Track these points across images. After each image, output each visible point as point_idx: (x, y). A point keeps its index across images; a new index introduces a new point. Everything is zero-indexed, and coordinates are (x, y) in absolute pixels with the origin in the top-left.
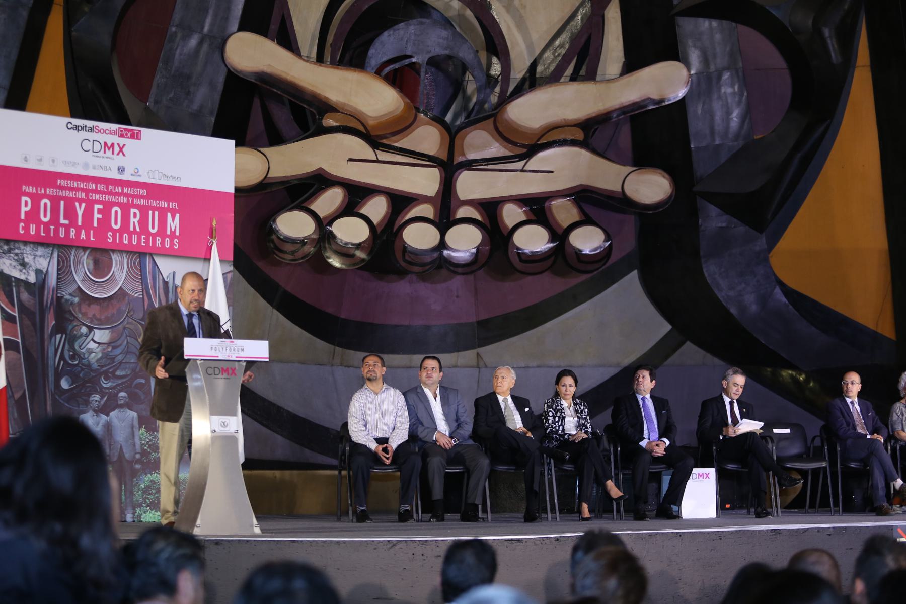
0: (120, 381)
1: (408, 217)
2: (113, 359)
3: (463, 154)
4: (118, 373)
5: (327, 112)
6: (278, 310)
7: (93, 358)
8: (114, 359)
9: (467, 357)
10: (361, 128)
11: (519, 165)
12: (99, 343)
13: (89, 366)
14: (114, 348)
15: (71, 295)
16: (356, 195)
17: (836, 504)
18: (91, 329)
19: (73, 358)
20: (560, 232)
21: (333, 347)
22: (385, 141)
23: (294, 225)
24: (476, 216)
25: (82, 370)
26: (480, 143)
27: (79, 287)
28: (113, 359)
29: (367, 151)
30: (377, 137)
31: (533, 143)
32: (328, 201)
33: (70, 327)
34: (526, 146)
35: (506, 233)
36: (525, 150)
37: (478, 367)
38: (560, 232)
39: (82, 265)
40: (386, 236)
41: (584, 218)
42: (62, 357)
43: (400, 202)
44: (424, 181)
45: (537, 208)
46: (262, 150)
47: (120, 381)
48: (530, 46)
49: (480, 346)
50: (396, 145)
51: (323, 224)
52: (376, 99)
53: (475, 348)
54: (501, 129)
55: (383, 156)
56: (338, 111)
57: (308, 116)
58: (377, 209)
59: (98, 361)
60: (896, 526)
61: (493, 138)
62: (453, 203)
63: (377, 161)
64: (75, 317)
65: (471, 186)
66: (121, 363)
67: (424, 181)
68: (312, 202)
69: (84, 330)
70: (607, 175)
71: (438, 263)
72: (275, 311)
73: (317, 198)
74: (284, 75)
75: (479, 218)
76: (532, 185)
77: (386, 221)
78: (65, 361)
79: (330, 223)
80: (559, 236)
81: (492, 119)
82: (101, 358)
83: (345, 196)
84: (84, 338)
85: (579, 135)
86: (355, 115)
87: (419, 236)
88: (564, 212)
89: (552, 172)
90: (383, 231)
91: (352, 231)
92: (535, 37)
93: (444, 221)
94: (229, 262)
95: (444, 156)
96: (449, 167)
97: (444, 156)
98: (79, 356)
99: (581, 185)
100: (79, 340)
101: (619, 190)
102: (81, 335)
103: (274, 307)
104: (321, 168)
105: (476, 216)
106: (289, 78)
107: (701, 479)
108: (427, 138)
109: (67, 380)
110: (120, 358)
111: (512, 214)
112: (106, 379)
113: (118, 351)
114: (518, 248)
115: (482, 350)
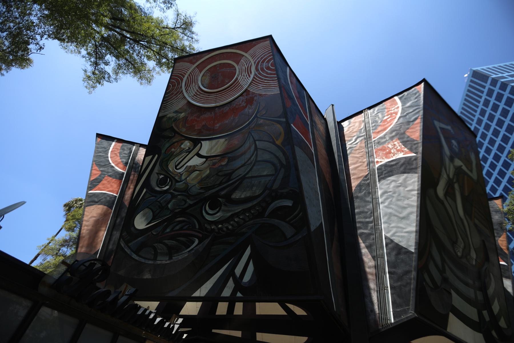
0: (239, 209)
2: (229, 176)
4: (236, 195)
7: (193, 179)
8: (231, 174)
13: (186, 191)
14: (231, 160)
15: (176, 112)
18: (196, 142)
19: (161, 183)
25: (173, 196)
27: (189, 102)
28: (229, 176)
33: (167, 145)
39: (196, 83)
47: (239, 209)
59: (202, 180)
64: (176, 132)
66: (244, 178)
69: (187, 144)
78: (151, 190)
82: (208, 177)
84: (184, 154)
98: (172, 179)
100: (176, 159)
102: (182, 151)
109: (144, 215)
110: (242, 172)
112: (211, 208)
113: (238, 163)
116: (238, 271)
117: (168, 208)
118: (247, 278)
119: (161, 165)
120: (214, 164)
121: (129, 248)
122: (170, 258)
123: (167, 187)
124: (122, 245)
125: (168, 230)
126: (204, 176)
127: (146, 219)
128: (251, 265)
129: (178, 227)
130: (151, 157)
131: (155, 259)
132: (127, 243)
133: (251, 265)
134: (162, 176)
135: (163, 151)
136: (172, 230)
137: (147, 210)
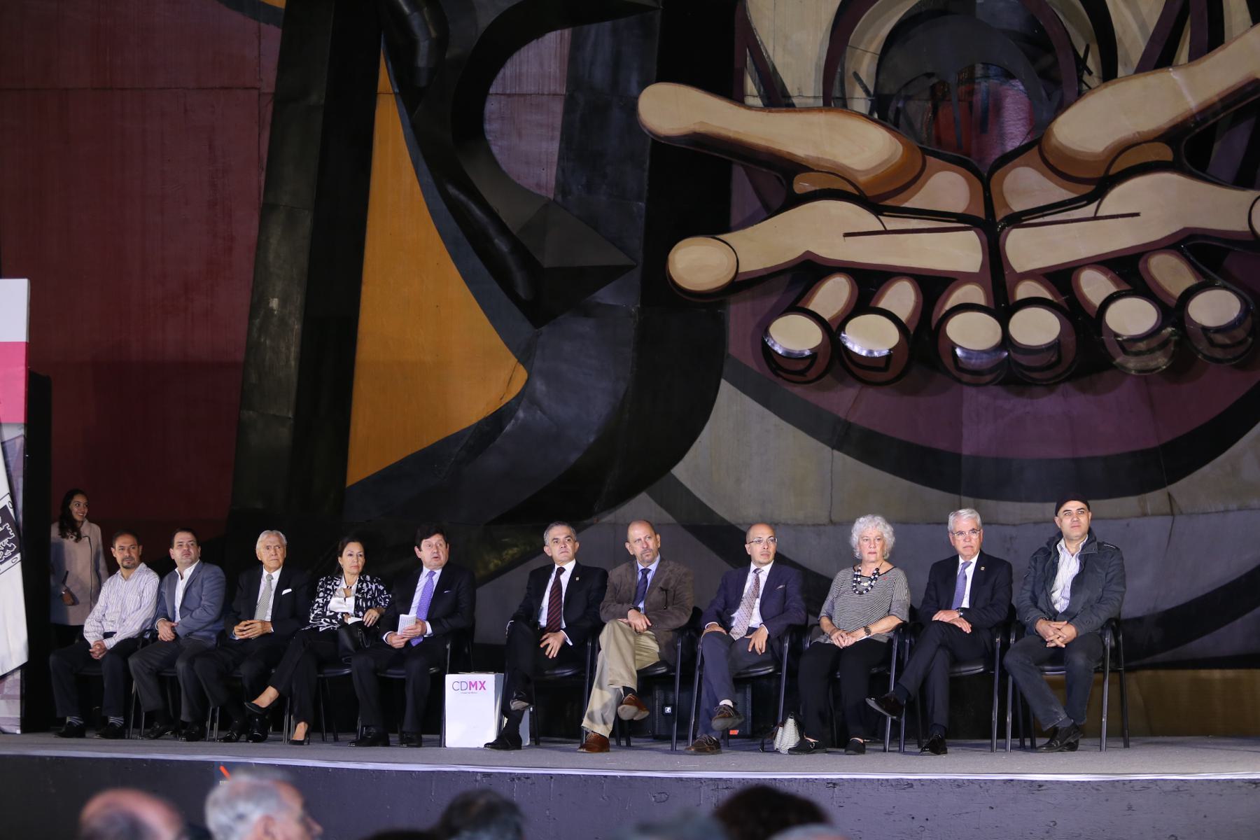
1: (948, 306)
3: (1007, 206)
5: (796, 174)
6: (839, 450)
9: (1156, 499)
10: (850, 189)
11: (1089, 210)
16: (869, 284)
17: (1002, 735)
20: (1173, 303)
21: (957, 497)
22: (889, 202)
23: (794, 335)
24: (1044, 293)
26: (1026, 185)
29: (868, 221)
30: (880, 198)
31: (1102, 174)
32: (832, 296)
34: (1094, 181)
35: (1094, 316)
36: (1093, 187)
37: (1172, 514)
38: (1173, 303)
40: (923, 337)
41: (1202, 280)
43: (932, 286)
44: (959, 252)
45: (1128, 270)
46: (722, 237)
48: (1142, 26)
49: (1171, 482)
50: (907, 205)
51: (833, 330)
52: (864, 146)
53: (1165, 486)
54: (1051, 160)
55: (893, 223)
56: (812, 170)
57: (782, 182)
58: (901, 299)
60: (219, 763)
61: (1044, 174)
62: (1008, 279)
63: (886, 232)
65: (1027, 249)
67: (959, 252)
68: (809, 300)
70: (1220, 208)
71: (1012, 369)
72: (836, 453)
73: (814, 293)
74: (724, 133)
75: (1048, 296)
76: (1118, 238)
77: (918, 315)
79: (842, 327)
80: (1173, 312)
81: (1036, 149)
83: (852, 287)
85: (1166, 153)
86: (837, 172)
87: (971, 333)
88: (1171, 273)
89: (1137, 215)
90: (917, 330)
91: (870, 338)
92: (1144, 10)
93: (1002, 307)
94: (18, 425)
95: (980, 213)
96: (990, 225)
97: (980, 213)
99: (1185, 230)
101: (1247, 229)
103: (833, 448)
104: (808, 252)
105: (1044, 293)
106: (731, 135)
107: (473, 689)
108: (948, 188)
111: (1094, 286)
114: (1117, 335)
115: (1172, 488)
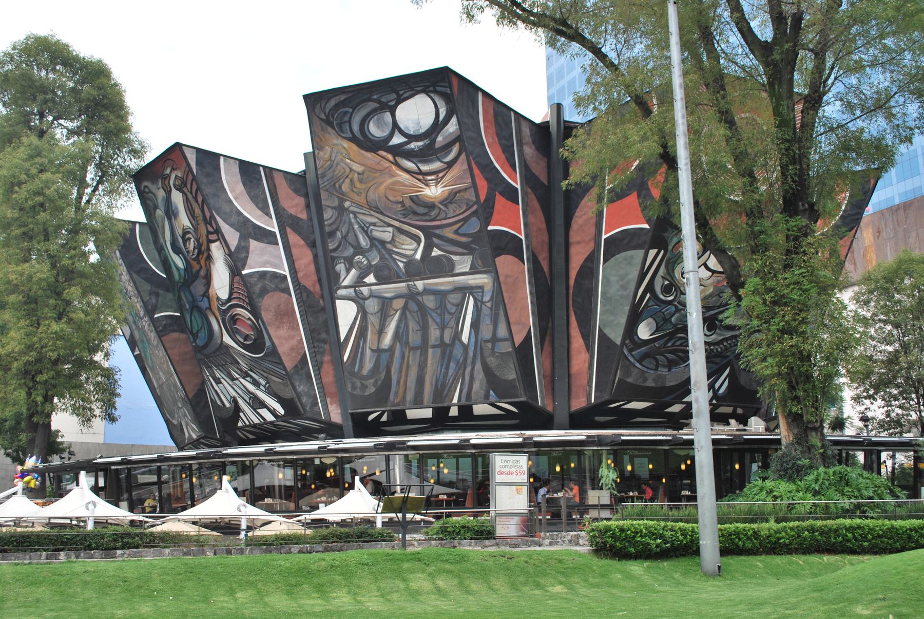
12: (713, 272)
19: (667, 290)
42: (650, 288)
78: (654, 296)
82: (711, 295)
109: (648, 325)
116: (717, 385)
117: (671, 322)
118: (721, 391)
119: (667, 267)
120: (719, 282)
121: (633, 356)
122: (669, 370)
123: (672, 298)
124: (626, 353)
125: (669, 344)
126: (707, 293)
127: (650, 329)
128: (727, 381)
129: (678, 343)
130: (656, 251)
131: (656, 369)
132: (630, 351)
133: (727, 381)
134: (667, 282)
135: (670, 248)
136: (673, 345)
137: (650, 320)
